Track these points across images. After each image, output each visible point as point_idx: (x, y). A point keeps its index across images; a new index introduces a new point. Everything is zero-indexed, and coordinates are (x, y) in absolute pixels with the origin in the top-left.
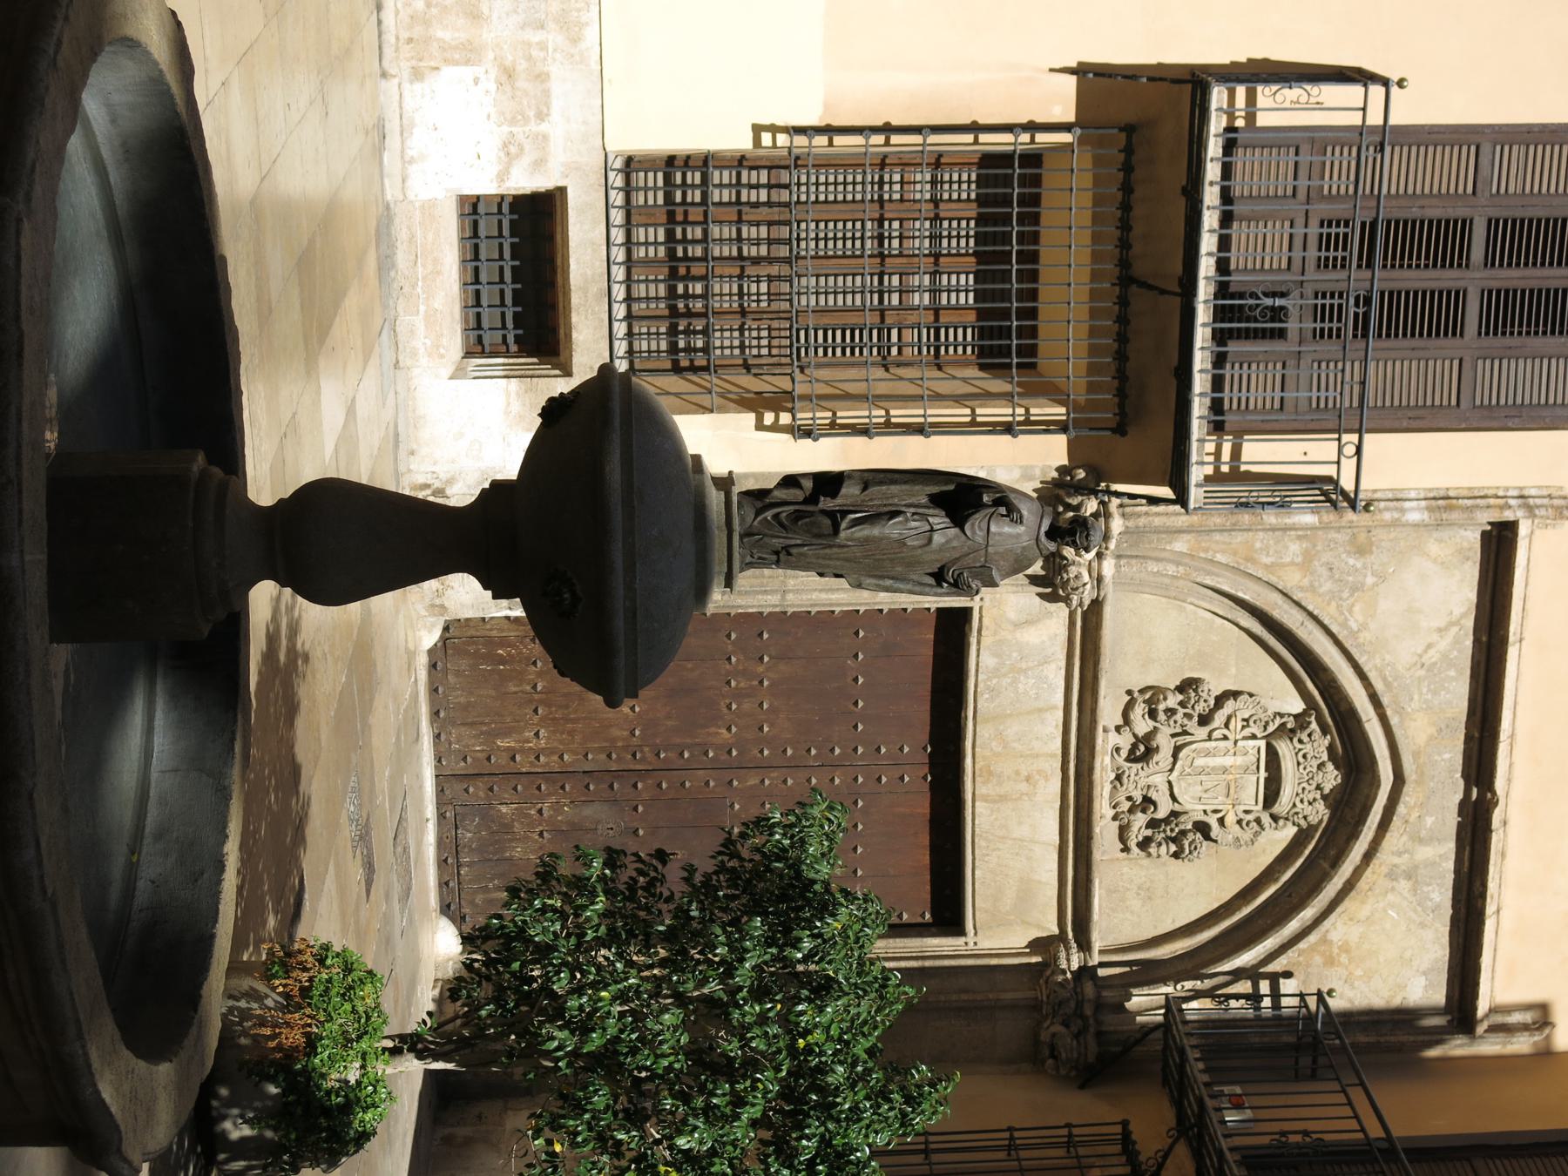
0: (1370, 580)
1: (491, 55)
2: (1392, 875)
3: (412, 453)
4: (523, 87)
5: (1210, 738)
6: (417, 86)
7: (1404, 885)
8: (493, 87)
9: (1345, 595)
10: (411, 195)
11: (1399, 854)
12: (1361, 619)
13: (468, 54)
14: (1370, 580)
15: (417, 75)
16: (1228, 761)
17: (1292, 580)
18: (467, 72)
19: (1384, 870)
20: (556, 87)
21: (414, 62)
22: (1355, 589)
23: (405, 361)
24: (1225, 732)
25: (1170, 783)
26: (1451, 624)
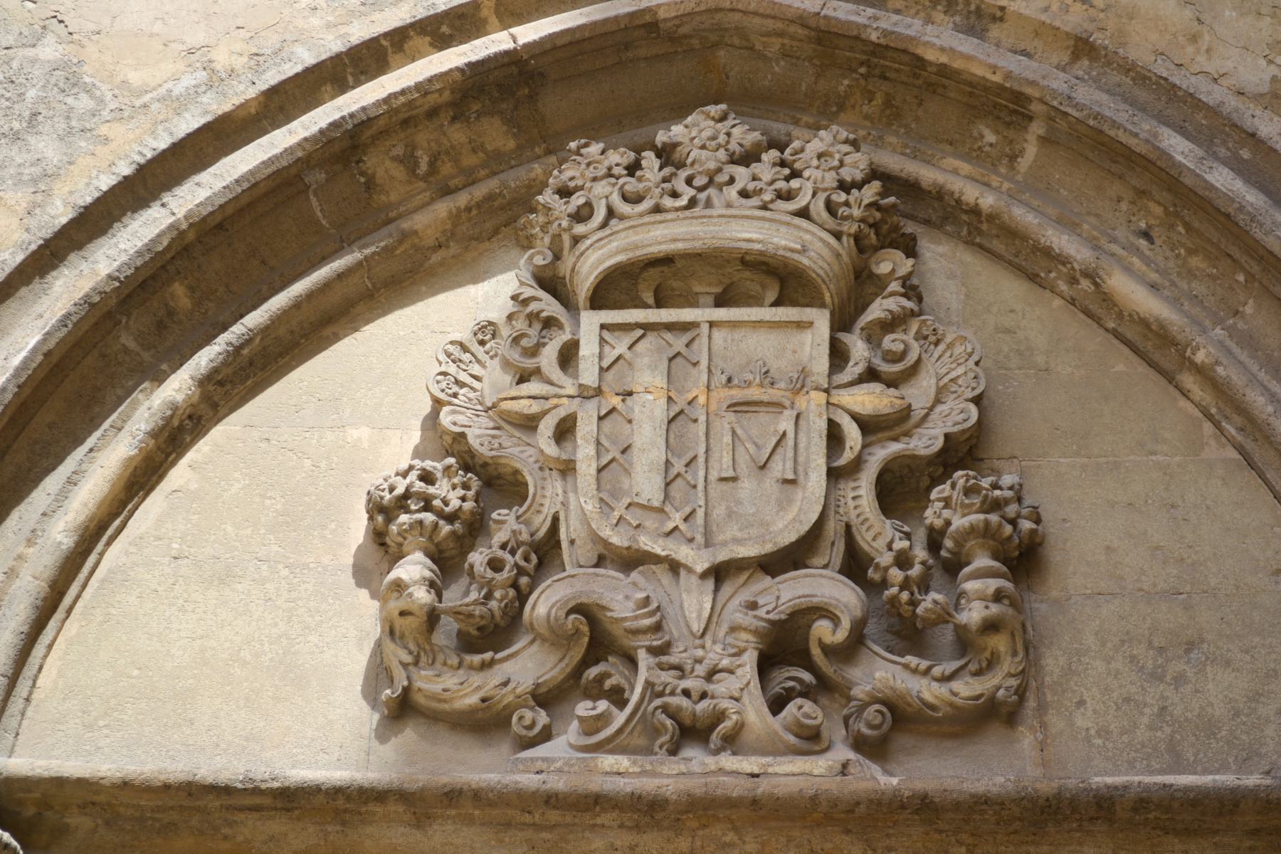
0: (49, 50)
5: (567, 469)
9: (83, 103)
14: (49, 50)
16: (649, 411)
24: (547, 427)
25: (719, 574)
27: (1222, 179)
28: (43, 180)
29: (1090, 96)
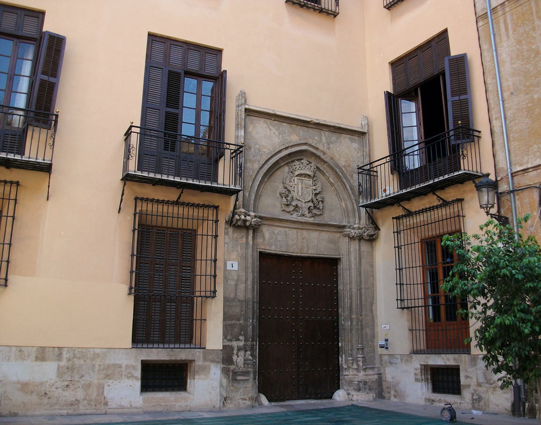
0: (257, 146)
1: (102, 381)
2: (329, 149)
3: (214, 407)
4: (111, 372)
6: (109, 404)
7: (331, 145)
8: (111, 381)
10: (141, 406)
11: (324, 146)
12: (267, 150)
13: (101, 388)
15: (106, 404)
17: (257, 166)
18: (106, 388)
19: (328, 150)
20: (112, 362)
21: (102, 404)
22: (260, 151)
23: (188, 409)
26: (269, 127)
27: (340, 174)
28: (259, 161)
29: (332, 164)
